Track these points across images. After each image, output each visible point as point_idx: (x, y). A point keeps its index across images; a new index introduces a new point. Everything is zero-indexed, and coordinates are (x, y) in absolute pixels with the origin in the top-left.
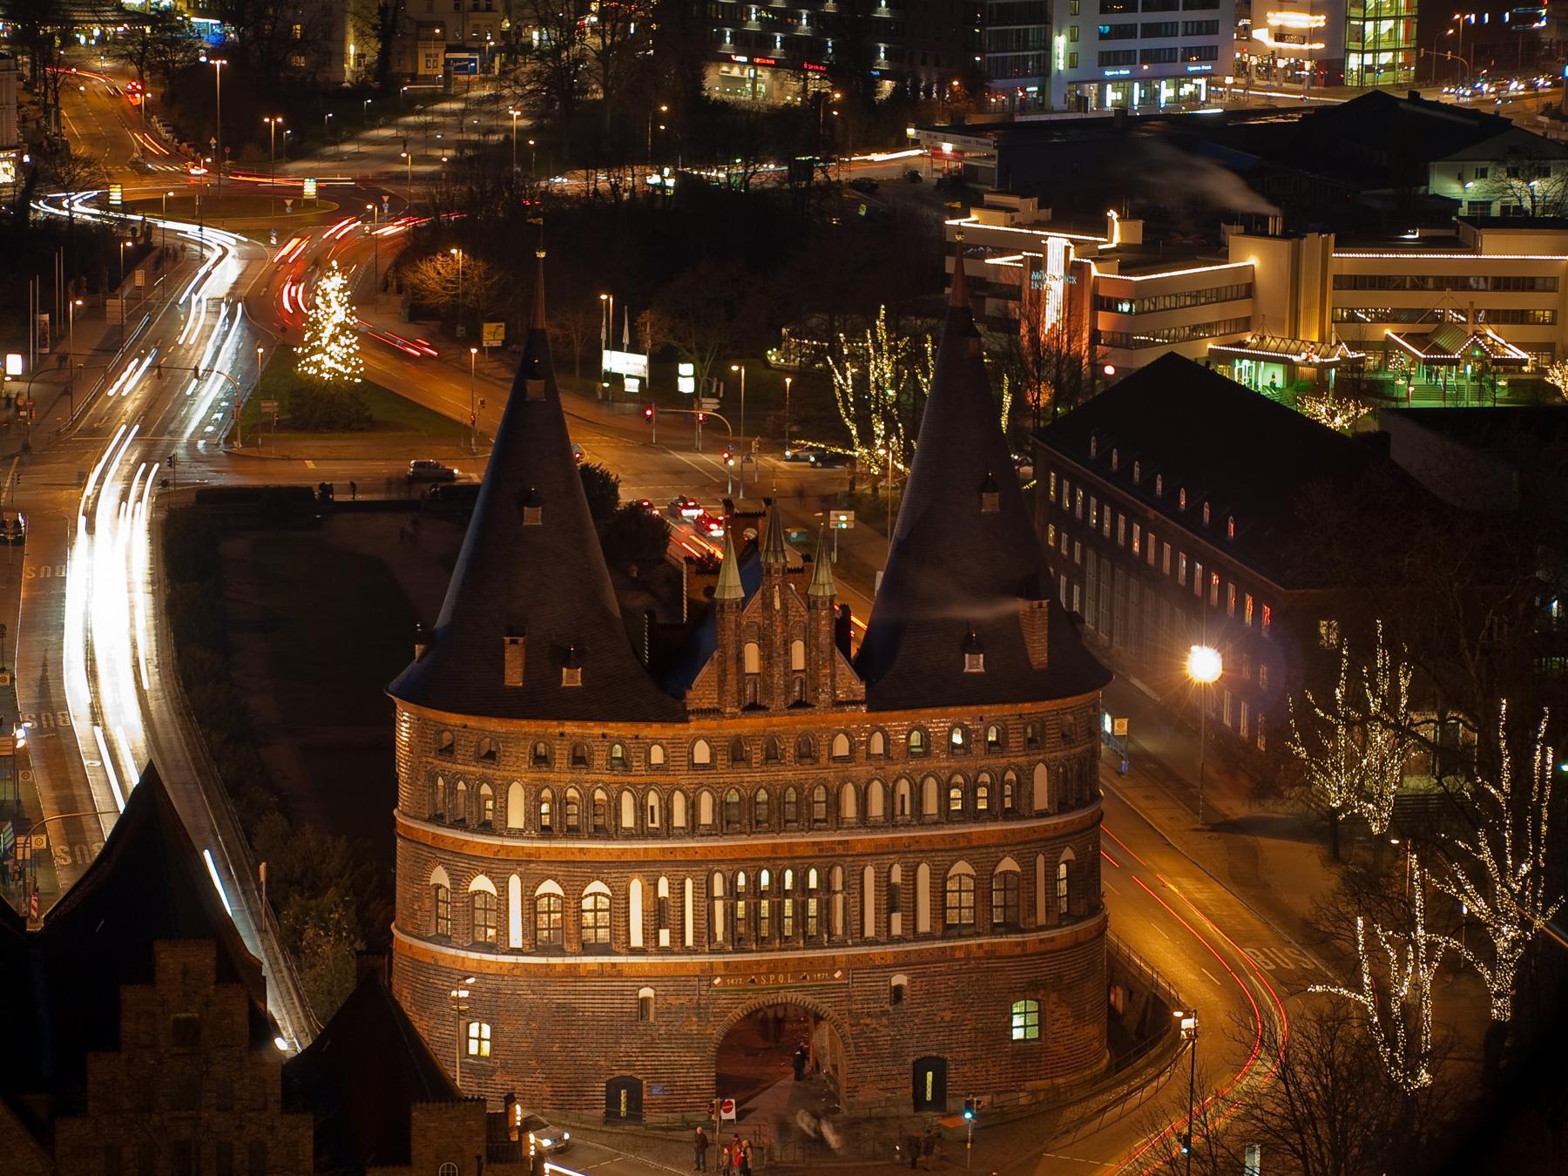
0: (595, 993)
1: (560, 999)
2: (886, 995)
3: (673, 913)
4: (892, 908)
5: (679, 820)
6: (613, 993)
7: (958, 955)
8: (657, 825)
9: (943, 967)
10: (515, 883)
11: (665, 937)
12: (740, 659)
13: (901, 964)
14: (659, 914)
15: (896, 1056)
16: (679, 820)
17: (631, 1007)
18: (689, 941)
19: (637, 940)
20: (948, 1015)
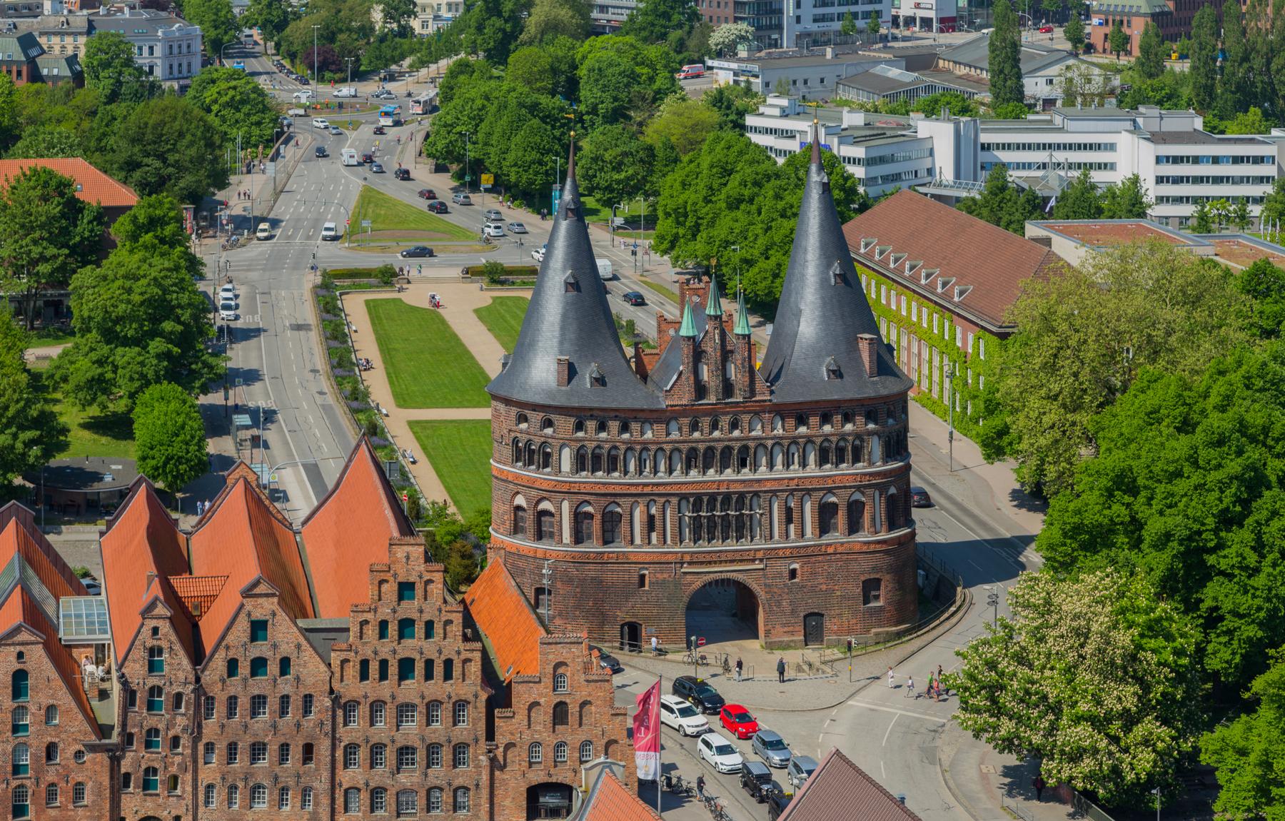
0: (612, 571)
1: (592, 574)
2: (786, 574)
3: (658, 523)
4: (789, 520)
5: (662, 467)
6: (624, 571)
7: (830, 550)
8: (648, 469)
9: (820, 558)
10: (566, 506)
11: (654, 535)
12: (696, 372)
13: (797, 554)
14: (650, 524)
15: (793, 612)
16: (662, 467)
17: (636, 579)
18: (669, 541)
19: (638, 541)
20: (824, 587)
